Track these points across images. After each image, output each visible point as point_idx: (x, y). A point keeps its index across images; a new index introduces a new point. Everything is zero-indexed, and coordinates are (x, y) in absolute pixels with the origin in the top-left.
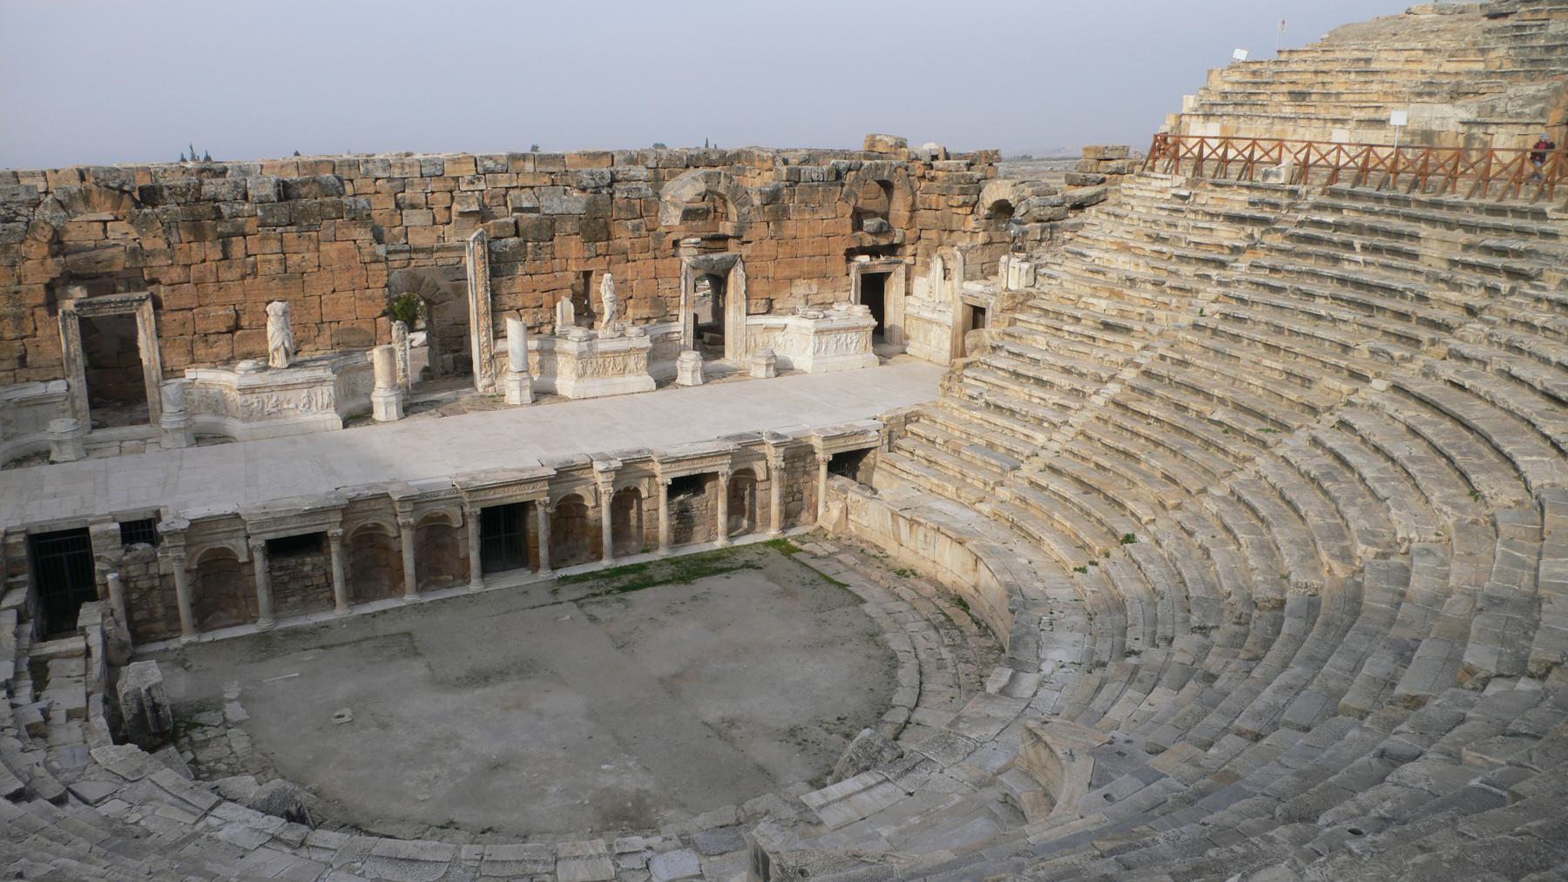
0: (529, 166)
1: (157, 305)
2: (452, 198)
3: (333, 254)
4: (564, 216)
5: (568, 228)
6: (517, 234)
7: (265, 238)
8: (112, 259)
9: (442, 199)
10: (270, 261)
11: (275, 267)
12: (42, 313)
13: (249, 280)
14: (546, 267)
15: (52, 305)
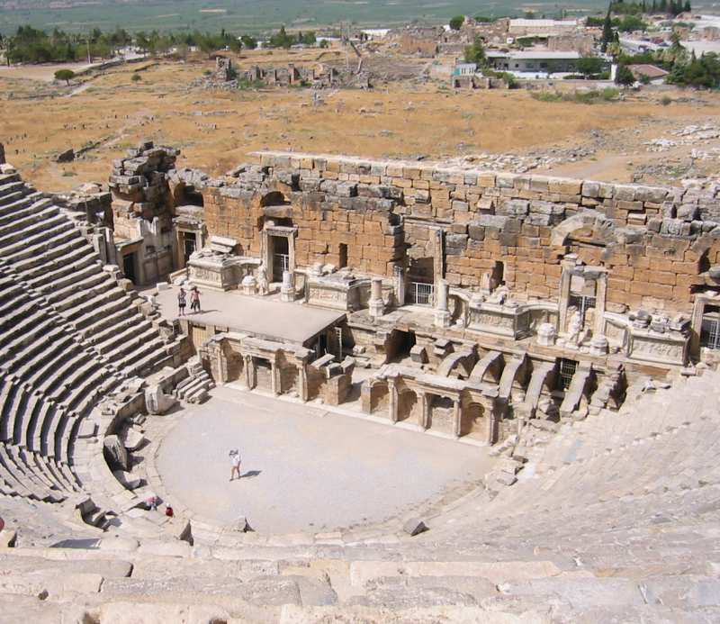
0: (527, 187)
1: (296, 235)
2: (480, 197)
3: (371, 227)
4: (491, 229)
5: (493, 235)
6: (467, 233)
7: (341, 214)
8: (281, 212)
9: (474, 197)
10: (342, 225)
11: (344, 229)
12: (256, 229)
13: (334, 231)
14: (477, 255)
15: (260, 226)
